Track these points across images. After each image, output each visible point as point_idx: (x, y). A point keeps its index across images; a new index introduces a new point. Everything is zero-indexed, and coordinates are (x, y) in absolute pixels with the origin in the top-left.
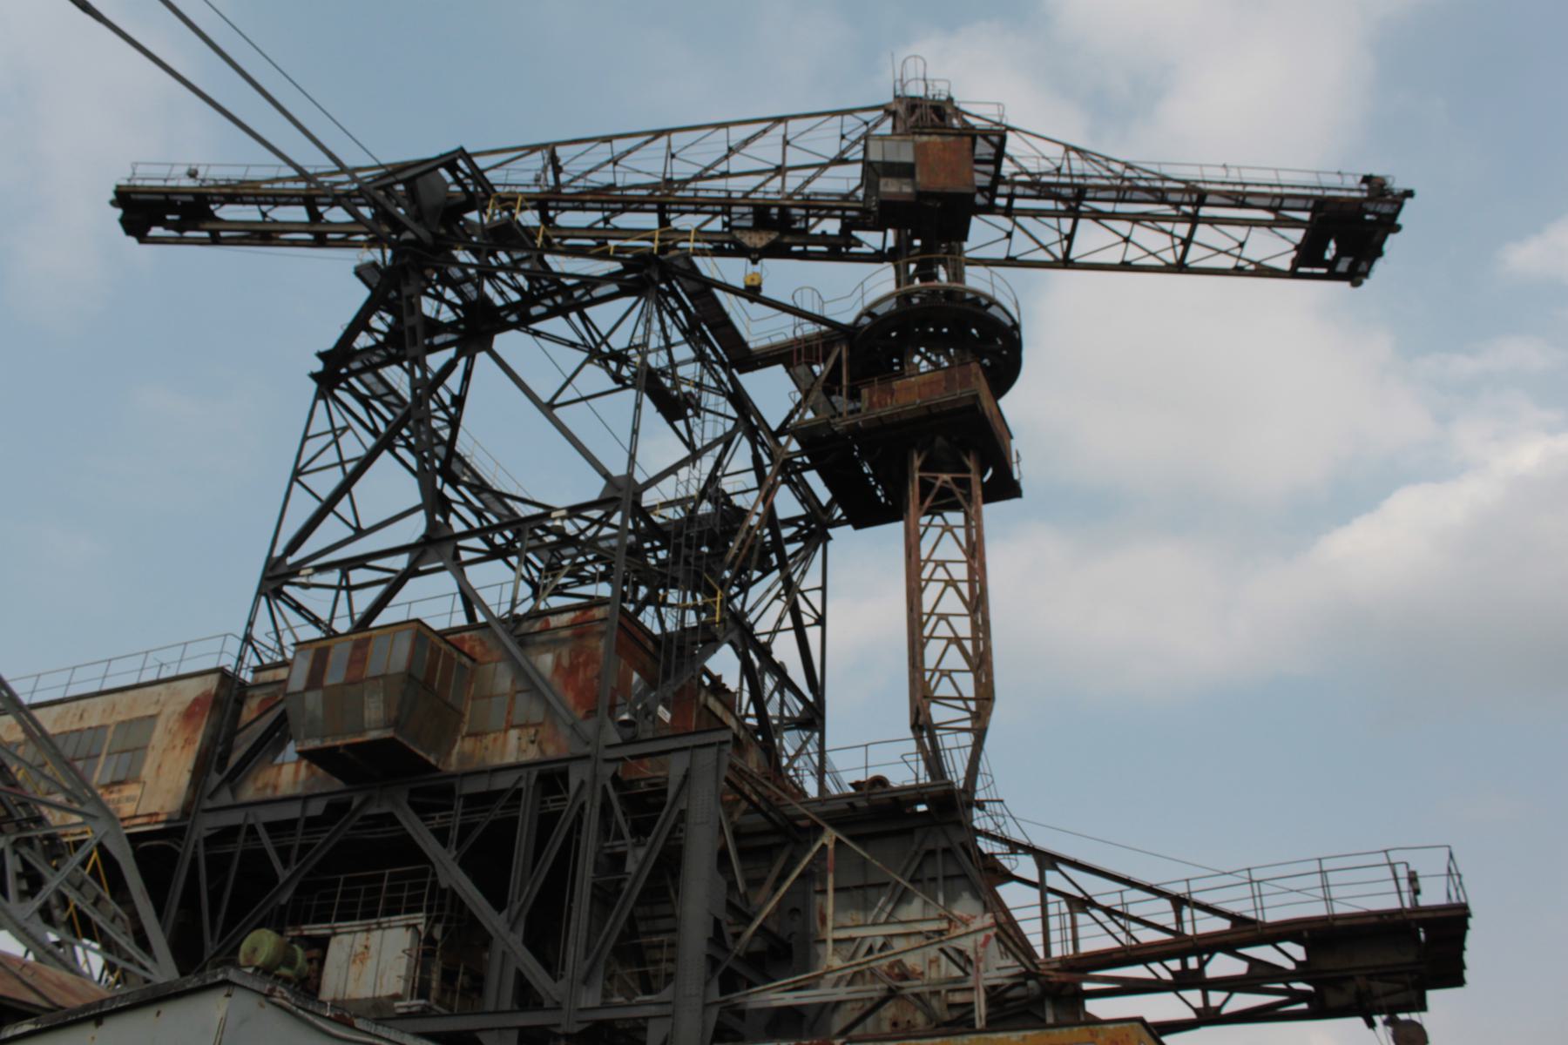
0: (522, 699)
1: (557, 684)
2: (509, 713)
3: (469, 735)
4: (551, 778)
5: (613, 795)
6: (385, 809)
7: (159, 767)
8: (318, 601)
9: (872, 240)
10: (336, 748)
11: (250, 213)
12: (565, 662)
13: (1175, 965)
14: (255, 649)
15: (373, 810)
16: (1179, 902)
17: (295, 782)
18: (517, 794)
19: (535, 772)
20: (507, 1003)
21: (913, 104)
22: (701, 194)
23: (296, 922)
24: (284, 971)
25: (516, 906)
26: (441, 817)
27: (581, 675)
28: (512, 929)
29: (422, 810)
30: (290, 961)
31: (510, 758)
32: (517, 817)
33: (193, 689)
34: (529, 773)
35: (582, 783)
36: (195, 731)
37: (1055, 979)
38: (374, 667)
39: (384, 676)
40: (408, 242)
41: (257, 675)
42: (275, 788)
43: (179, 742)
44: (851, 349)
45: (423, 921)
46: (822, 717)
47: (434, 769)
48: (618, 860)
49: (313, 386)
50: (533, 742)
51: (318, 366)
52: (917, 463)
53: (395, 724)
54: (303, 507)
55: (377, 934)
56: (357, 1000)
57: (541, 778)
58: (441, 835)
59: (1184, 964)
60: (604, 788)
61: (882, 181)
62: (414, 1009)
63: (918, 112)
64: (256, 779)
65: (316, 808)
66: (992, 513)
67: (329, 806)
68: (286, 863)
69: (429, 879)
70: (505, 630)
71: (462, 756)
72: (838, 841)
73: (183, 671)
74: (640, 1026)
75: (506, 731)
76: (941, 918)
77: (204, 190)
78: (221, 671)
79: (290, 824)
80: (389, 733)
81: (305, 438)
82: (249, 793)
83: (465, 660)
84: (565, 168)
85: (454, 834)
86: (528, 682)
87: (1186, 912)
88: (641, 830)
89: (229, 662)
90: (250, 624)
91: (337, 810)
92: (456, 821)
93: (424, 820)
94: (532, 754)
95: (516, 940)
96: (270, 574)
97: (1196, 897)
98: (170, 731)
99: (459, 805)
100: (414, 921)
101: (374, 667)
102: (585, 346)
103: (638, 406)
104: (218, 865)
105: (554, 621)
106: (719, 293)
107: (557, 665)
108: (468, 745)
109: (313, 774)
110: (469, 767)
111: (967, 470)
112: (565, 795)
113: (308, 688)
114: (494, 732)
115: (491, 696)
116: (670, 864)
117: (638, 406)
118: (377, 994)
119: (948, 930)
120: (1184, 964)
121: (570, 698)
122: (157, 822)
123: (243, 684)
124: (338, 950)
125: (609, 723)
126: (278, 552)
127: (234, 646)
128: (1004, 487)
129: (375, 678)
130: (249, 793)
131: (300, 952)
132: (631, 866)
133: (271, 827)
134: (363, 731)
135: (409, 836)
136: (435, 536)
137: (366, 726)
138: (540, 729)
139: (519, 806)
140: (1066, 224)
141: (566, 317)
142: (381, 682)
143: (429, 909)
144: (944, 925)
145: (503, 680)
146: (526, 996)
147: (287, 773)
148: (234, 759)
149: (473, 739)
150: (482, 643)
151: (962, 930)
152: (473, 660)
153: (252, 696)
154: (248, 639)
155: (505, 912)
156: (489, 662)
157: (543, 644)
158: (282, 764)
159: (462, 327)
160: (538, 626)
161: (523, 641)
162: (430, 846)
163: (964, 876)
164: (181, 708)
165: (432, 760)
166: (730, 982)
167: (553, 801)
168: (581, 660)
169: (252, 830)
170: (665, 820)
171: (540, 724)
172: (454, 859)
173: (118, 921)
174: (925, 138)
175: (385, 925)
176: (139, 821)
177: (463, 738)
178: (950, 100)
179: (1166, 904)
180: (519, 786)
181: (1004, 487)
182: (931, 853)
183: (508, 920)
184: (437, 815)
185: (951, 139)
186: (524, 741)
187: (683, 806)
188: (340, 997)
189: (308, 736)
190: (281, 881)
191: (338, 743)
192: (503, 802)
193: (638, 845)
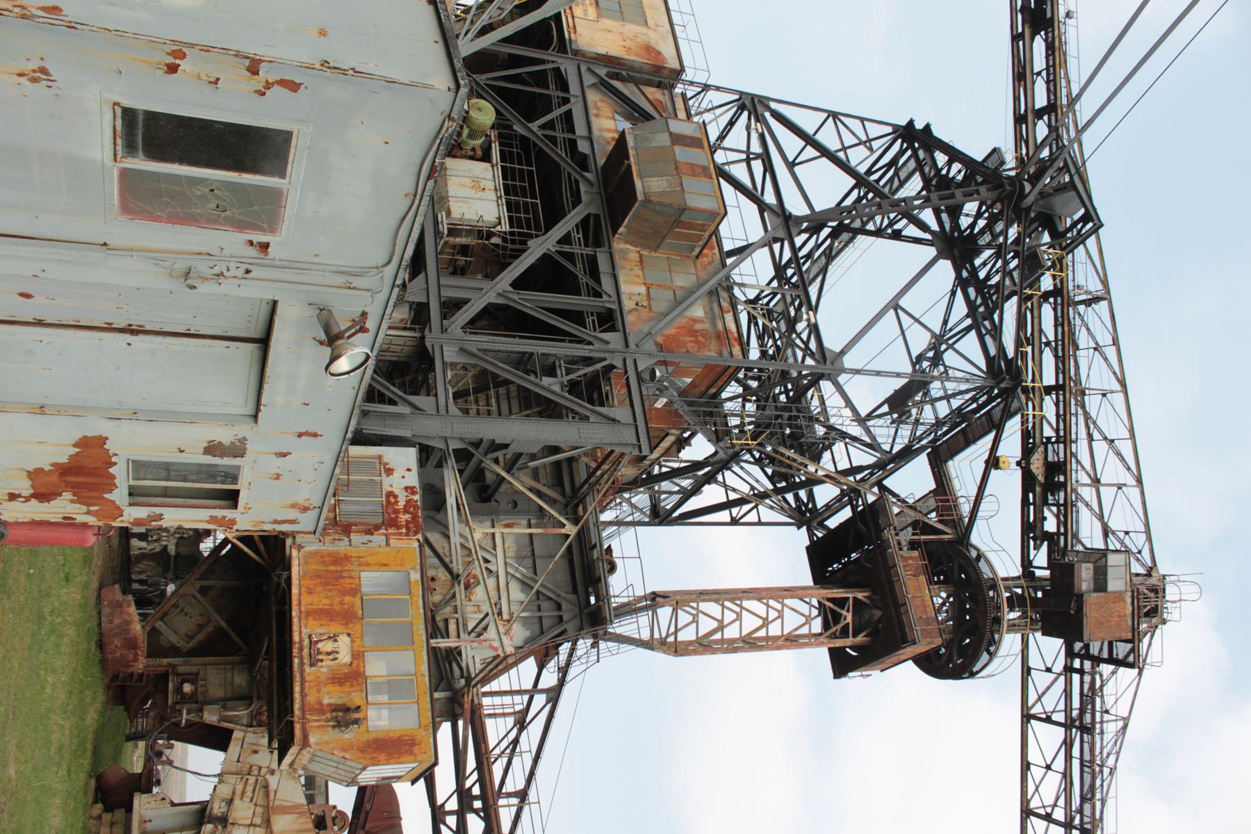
0: (669, 295)
1: (682, 321)
2: (659, 286)
3: (641, 256)
4: (609, 320)
5: (598, 366)
6: (584, 197)
7: (610, 31)
8: (737, 138)
9: (1040, 557)
10: (628, 158)
11: (1039, 62)
12: (698, 327)
13: (476, 791)
14: (699, 93)
15: (583, 188)
16: (522, 795)
18: (598, 295)
19: (614, 307)
20: (447, 293)
21: (1158, 591)
22: (1073, 419)
23: (500, 136)
24: (466, 132)
25: (515, 297)
26: (579, 238)
27: (690, 339)
28: (499, 294)
29: (584, 224)
30: (472, 136)
31: (624, 288)
32: (581, 295)
33: (668, 51)
34: (614, 302)
35: (607, 343)
36: (637, 55)
37: (466, 700)
38: (689, 182)
39: (683, 189)
40: (1022, 188)
41: (680, 97)
42: (597, 116)
43: (624, 44)
44: (950, 542)
45: (504, 230)
46: (660, 524)
47: (615, 232)
48: (551, 371)
49: (903, 123)
50: (637, 304)
51: (919, 125)
52: (860, 596)
53: (647, 201)
54: (808, 122)
56: (446, 185)
57: (610, 311)
58: (566, 240)
59: (476, 798)
60: (605, 359)
61: (1091, 566)
62: (440, 226)
63: (1152, 595)
64: (602, 101)
65: (583, 147)
66: (820, 657)
67: (585, 155)
68: (543, 127)
69: (533, 232)
70: (721, 280)
71: (622, 251)
72: (567, 536)
73: (681, 43)
74: (430, 391)
75: (645, 284)
76: (511, 614)
77: (1056, 25)
78: (682, 70)
79: (572, 130)
80: (640, 196)
81: (862, 120)
82: (593, 97)
83: (697, 250)
84: (1090, 309)
85: (566, 248)
86: (681, 300)
87: (515, 801)
88: (573, 388)
89: (689, 75)
90: (718, 88)
91: (582, 162)
92: (576, 250)
93: (577, 226)
94: (628, 304)
95: (491, 298)
96: (756, 100)
97: (526, 809)
99: (588, 251)
100: (503, 223)
101: (689, 182)
102: (945, 332)
103: (898, 375)
104: (540, 79)
105: (729, 317)
106: (991, 436)
107: (695, 321)
108: (634, 256)
109: (608, 143)
110: (616, 256)
111: (855, 636)
112: (598, 330)
113: (671, 134)
114: (643, 275)
115: (670, 271)
116: (549, 410)
117: (898, 375)
118: (450, 199)
119: (502, 619)
120: (476, 798)
121: (671, 331)
122: (569, 32)
123: (673, 87)
124: (482, 170)
125: (654, 361)
126: (773, 105)
127: (701, 78)
128: (842, 665)
129: (681, 184)
130: (593, 97)
131: (479, 142)
132: (546, 381)
133: (569, 115)
134: (641, 177)
135: (565, 215)
136: (790, 223)
137: (645, 179)
138: (647, 310)
139: (589, 296)
140: (1060, 717)
141: (967, 316)
142: (678, 189)
143: (512, 234)
144: (505, 616)
145: (682, 280)
146: (451, 307)
147: (610, 124)
148: (617, 84)
149: (638, 259)
150: (710, 263)
151: (502, 630)
152: (697, 257)
153: (664, 94)
154: (706, 87)
155: (511, 289)
156: (696, 269)
157: (711, 309)
158: (615, 120)
159: (956, 234)
160: (725, 304)
161: (713, 293)
162: (558, 232)
163: (542, 633)
164: (653, 43)
165: (621, 230)
166: (463, 456)
167: (593, 321)
168: (700, 338)
169: (566, 101)
170: (581, 406)
171: (650, 309)
172: (549, 249)
173: (500, 12)
174: (1129, 600)
175: (500, 201)
177: (639, 252)
178: (1164, 622)
179: (521, 785)
180: (604, 296)
181: (842, 665)
182: (559, 607)
183: (504, 291)
184: (581, 236)
185: (1130, 623)
186: (638, 298)
187: (591, 420)
188: (448, 172)
189: (635, 137)
190: (529, 125)
191: (632, 159)
192: (592, 284)
193: (562, 384)
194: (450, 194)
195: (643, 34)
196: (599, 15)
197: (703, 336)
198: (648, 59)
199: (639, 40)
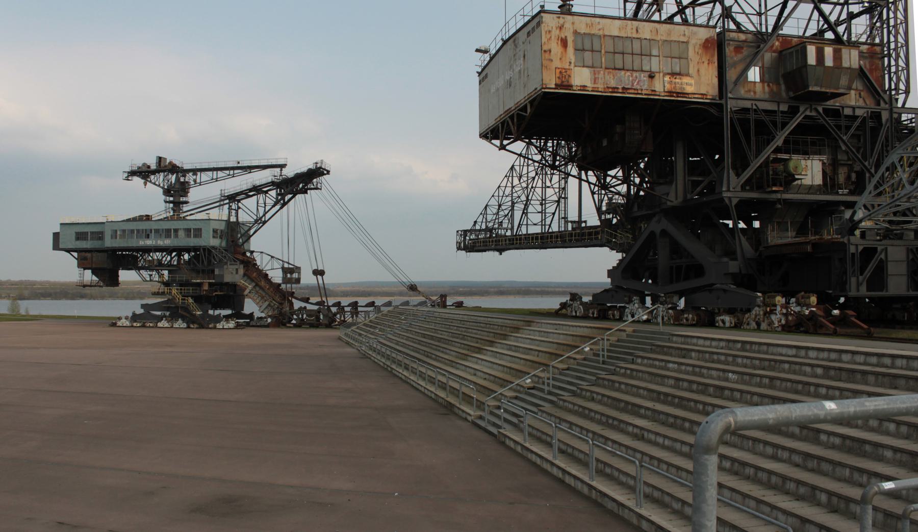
7: (698, 71)
10: (827, 93)
15: (808, 113)
17: (764, 92)
42: (755, 93)
43: (706, 63)
55: (809, 162)
56: (805, 185)
98: (698, 53)
99: (843, 118)
113: (817, 65)
122: (706, 99)
142: (849, 71)
164: (699, 42)
176: (696, 96)
194: (811, 184)
195: (695, 47)
196: (688, 75)
197: (872, 65)
198: (714, 49)
199: (700, 51)
